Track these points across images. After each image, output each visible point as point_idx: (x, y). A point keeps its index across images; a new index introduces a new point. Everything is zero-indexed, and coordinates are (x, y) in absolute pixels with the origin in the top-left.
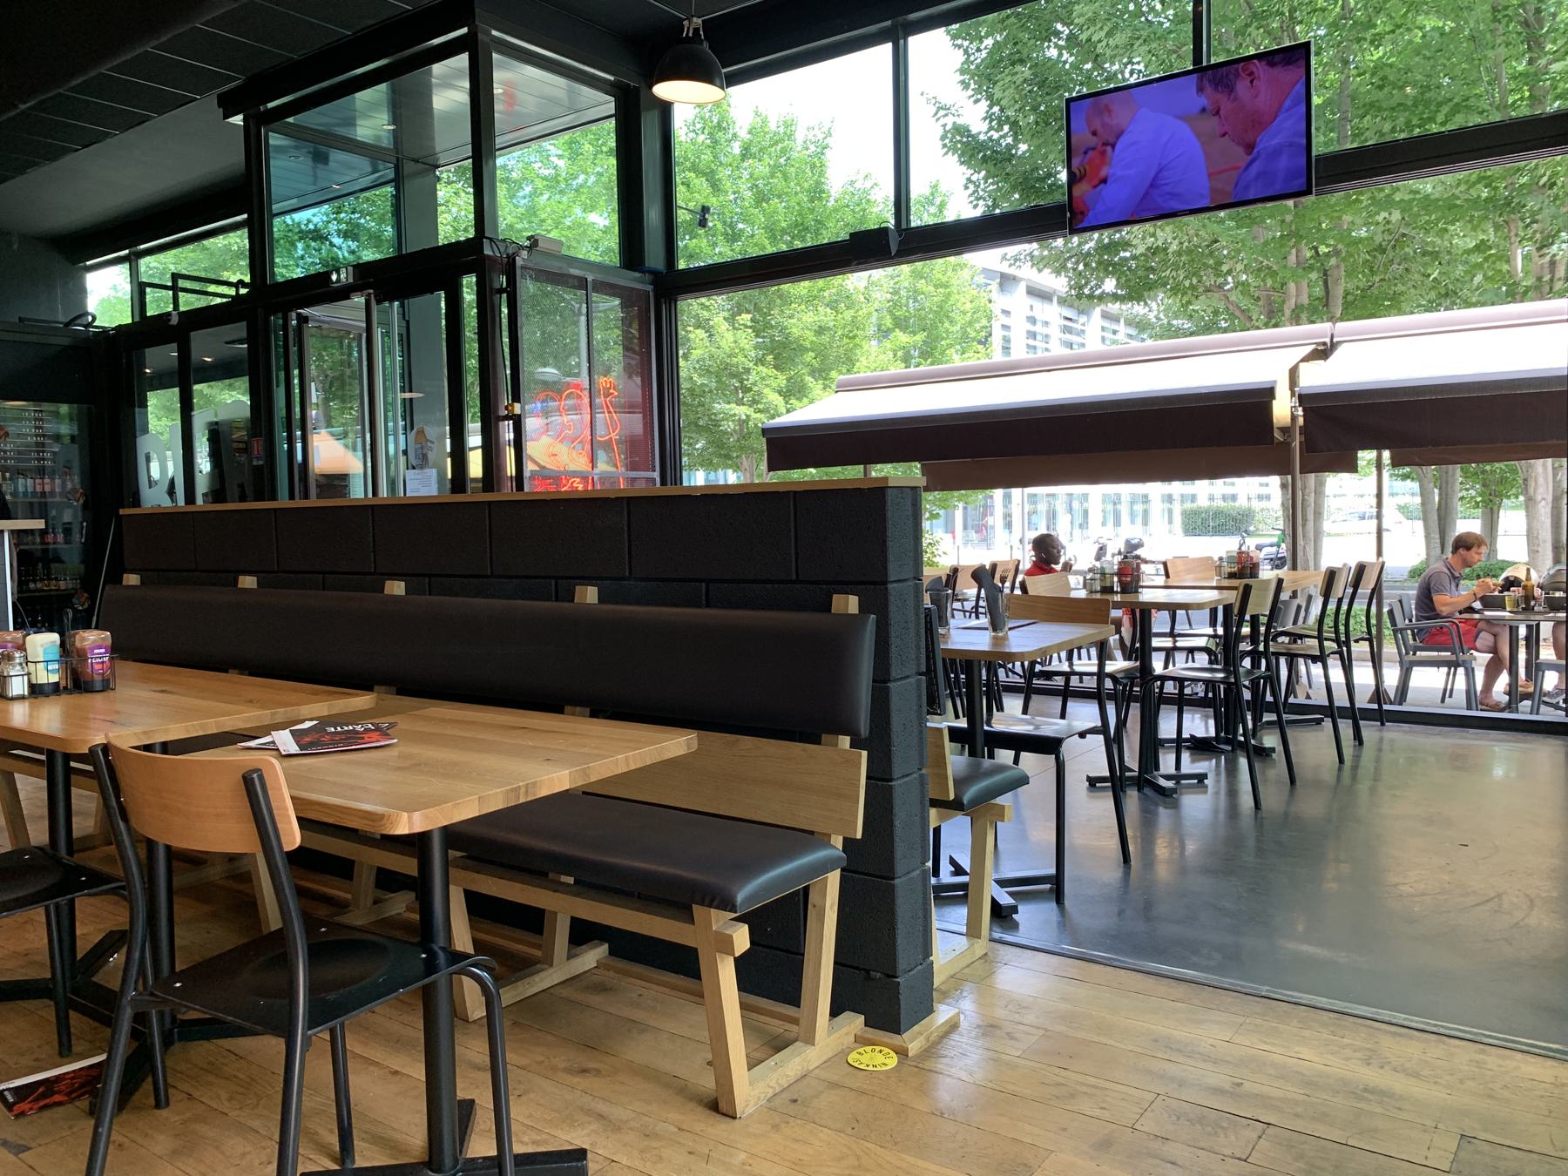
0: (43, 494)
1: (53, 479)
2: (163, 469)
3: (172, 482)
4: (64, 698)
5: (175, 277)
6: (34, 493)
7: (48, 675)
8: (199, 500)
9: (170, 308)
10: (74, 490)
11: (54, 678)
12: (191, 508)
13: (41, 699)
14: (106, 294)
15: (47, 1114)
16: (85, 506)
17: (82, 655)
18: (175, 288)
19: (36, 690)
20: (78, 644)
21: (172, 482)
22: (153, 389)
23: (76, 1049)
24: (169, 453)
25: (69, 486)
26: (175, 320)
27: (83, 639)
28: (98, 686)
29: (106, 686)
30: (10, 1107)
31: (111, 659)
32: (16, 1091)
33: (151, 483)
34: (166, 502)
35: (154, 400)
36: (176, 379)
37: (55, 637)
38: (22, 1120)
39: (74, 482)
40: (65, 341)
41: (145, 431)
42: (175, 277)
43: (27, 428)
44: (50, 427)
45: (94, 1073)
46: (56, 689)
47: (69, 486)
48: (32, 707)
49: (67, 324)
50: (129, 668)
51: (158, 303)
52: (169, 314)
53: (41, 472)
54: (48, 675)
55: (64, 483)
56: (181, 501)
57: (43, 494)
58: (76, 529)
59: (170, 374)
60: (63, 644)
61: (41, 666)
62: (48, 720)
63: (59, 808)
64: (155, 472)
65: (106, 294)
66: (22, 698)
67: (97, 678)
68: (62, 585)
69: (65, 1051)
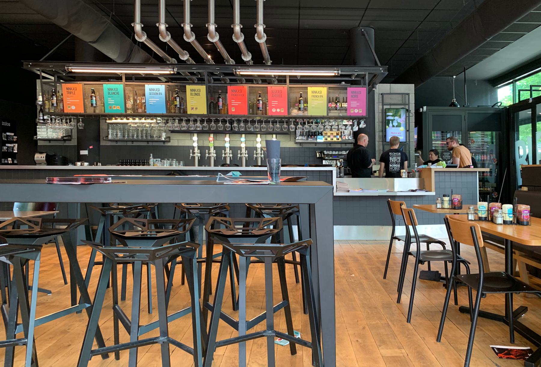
0: (484, 160)
1: (487, 156)
2: (525, 151)
3: (528, 156)
4: (514, 226)
5: (531, 86)
6: (481, 160)
7: (509, 218)
8: (538, 163)
9: (529, 97)
10: (493, 159)
11: (511, 219)
12: (534, 166)
13: (507, 226)
14: (505, 96)
15: (509, 360)
16: (497, 164)
17: (520, 213)
18: (531, 90)
19: (505, 222)
20: (519, 209)
21: (528, 156)
22: (521, 125)
23: (516, 342)
24: (527, 146)
25: (492, 158)
26: (531, 101)
27: (521, 208)
28: (525, 223)
29: (527, 224)
30: (497, 354)
31: (530, 215)
32: (498, 349)
33: (520, 157)
34: (526, 164)
35: (522, 128)
36: (530, 121)
37: (510, 206)
38: (501, 359)
39: (494, 156)
40: (492, 112)
41: (518, 139)
42: (531, 86)
43: (480, 140)
44: (486, 139)
45: (524, 352)
46: (511, 223)
47: (492, 158)
48: (504, 227)
49: (493, 106)
50: (533, 218)
51: (525, 96)
52: (529, 99)
53: (483, 153)
54: (509, 218)
55: (490, 157)
56: (531, 163)
57: (484, 160)
58: (493, 172)
59: (528, 119)
60: (514, 209)
61: (507, 215)
62: (509, 232)
63: (510, 262)
64: (521, 153)
65: (505, 96)
66: (501, 224)
67: (525, 221)
68: (489, 189)
69: (512, 341)
